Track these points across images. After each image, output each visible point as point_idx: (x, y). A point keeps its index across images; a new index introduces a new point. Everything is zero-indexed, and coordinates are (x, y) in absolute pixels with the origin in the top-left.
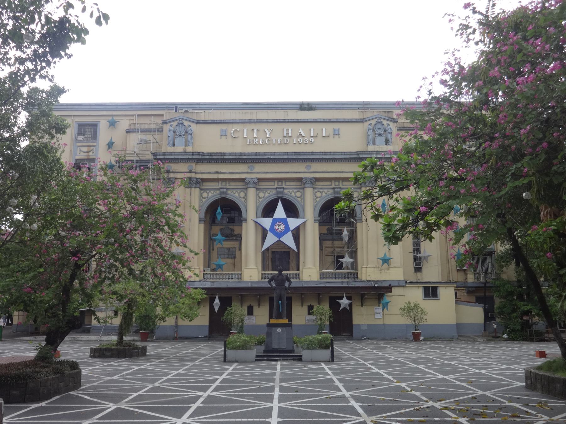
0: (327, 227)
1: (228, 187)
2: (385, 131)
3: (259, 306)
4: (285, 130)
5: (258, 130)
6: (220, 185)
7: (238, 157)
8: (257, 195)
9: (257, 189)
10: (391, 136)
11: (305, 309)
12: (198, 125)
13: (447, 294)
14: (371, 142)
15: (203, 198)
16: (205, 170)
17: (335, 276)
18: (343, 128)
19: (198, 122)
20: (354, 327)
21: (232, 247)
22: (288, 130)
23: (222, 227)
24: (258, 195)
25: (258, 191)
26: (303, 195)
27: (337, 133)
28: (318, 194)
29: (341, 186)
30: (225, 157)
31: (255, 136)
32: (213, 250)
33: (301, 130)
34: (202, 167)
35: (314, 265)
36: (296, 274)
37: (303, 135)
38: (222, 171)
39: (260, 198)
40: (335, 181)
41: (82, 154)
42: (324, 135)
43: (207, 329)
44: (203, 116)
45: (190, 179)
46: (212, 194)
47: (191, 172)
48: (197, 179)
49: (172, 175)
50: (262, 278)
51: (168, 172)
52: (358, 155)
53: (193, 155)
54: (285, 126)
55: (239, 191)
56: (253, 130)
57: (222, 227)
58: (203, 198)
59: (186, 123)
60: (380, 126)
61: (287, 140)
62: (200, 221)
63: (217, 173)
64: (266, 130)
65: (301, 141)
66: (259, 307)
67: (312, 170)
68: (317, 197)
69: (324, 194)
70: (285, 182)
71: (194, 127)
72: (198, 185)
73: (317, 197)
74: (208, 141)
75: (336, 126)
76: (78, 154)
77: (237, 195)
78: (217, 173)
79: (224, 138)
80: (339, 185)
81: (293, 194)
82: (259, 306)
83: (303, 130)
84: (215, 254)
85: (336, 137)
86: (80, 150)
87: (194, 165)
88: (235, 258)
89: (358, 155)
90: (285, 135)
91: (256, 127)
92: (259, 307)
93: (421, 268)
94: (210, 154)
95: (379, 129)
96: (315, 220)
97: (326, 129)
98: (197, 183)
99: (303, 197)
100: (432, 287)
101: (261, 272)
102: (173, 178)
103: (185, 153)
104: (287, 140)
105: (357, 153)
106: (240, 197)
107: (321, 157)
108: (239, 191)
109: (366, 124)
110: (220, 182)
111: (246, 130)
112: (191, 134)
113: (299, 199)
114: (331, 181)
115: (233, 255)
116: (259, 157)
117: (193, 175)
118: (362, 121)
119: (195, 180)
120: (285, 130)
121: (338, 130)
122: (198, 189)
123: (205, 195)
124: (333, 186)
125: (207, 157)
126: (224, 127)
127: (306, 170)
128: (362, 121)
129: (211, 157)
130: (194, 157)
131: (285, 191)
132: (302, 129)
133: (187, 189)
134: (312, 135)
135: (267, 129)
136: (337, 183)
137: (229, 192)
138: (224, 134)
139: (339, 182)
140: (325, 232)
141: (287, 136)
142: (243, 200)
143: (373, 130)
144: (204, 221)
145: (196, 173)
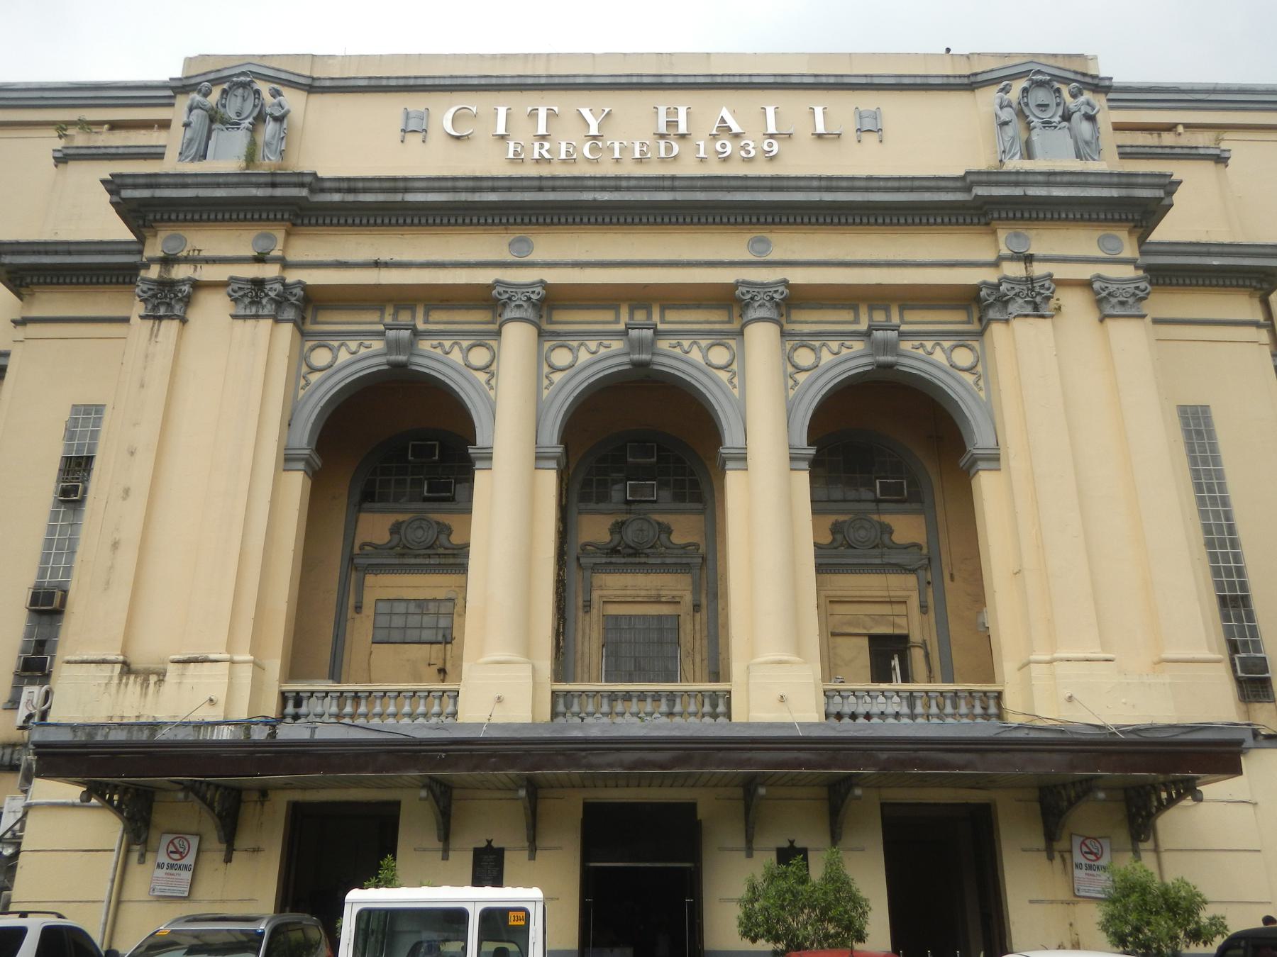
0: (833, 518)
1: (421, 326)
2: (1067, 117)
3: (533, 849)
4: (662, 110)
5: (551, 115)
6: (388, 319)
7: (463, 197)
8: (542, 358)
9: (541, 334)
10: (1096, 130)
12: (318, 100)
14: (1017, 148)
15: (314, 370)
16: (328, 259)
18: (891, 106)
21: (441, 594)
22: (672, 112)
23: (401, 517)
24: (547, 359)
25: (547, 345)
27: (870, 128)
28: (804, 357)
29: (895, 319)
30: (411, 197)
31: (542, 130)
32: (358, 608)
33: (725, 113)
34: (309, 247)
35: (798, 650)
36: (714, 696)
37: (736, 129)
38: (397, 258)
39: (555, 369)
40: (872, 308)
42: (820, 129)
45: (259, 284)
46: (352, 354)
47: (260, 259)
48: (284, 285)
49: (180, 272)
50: (554, 714)
51: (168, 261)
52: (968, 189)
53: (274, 185)
54: (663, 101)
55: (465, 344)
56: (533, 114)
57: (401, 517)
58: (314, 370)
60: (1041, 96)
61: (669, 149)
62: (288, 459)
63: (377, 264)
64: (586, 112)
65: (729, 150)
66: (532, 857)
67: (775, 255)
68: (800, 370)
69: (826, 357)
70: (663, 309)
71: (293, 100)
72: (290, 313)
73: (800, 370)
74: (344, 144)
75: (868, 101)
77: (456, 356)
78: (377, 264)
79: (414, 140)
80: (888, 318)
81: (696, 355)
82: (533, 849)
83: (734, 112)
84: (361, 629)
85: (870, 139)
88: (447, 639)
89: (968, 189)
90: (663, 129)
91: (543, 104)
92: (532, 857)
93: (1266, 683)
94: (350, 185)
95: (1043, 107)
96: (792, 459)
97: (822, 112)
98: (280, 302)
99: (737, 366)
101: (548, 686)
102: (183, 282)
104: (669, 149)
105: (967, 181)
106: (468, 366)
107: (815, 197)
108: (465, 344)
109: (988, 98)
110: (389, 311)
111: (500, 112)
112: (279, 119)
113: (724, 376)
114: (855, 308)
115: (439, 631)
116: (551, 196)
117: (269, 271)
118: (970, 84)
119: (278, 287)
120: (662, 110)
121: (875, 116)
122: (287, 330)
123: (321, 357)
124: (863, 326)
125: (337, 197)
126: (416, 103)
129: (350, 198)
130: (279, 192)
131: (664, 345)
132: (727, 110)
133: (240, 322)
134: (772, 129)
135: (590, 110)
136: (879, 317)
137: (425, 345)
138: (414, 128)
139: (887, 309)
140: (827, 539)
141: (671, 133)
142: (482, 377)
143: (1021, 114)
144: (308, 462)
145: (285, 264)
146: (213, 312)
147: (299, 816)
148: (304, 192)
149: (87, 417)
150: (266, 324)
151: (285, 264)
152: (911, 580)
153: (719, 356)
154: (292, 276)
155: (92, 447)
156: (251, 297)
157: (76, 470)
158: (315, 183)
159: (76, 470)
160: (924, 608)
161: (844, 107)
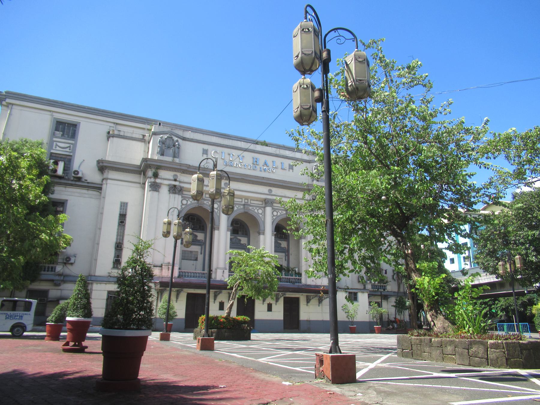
11: (265, 307)
13: (363, 297)
17: (289, 281)
19: (184, 139)
20: (301, 323)
21: (196, 250)
26: (264, 212)
41: (58, 148)
43: (184, 322)
44: (189, 135)
45: (175, 186)
47: (175, 180)
49: (158, 181)
59: (175, 139)
67: (273, 193)
73: (274, 216)
76: (54, 148)
85: (291, 170)
86: (57, 145)
87: (178, 174)
100: (354, 293)
103: (173, 162)
113: (261, 216)
117: (177, 183)
118: (309, 162)
126: (206, 147)
127: (268, 193)
128: (309, 162)
145: (180, 182)
146: (164, 190)
147: (189, 296)
148: (186, 168)
149: (124, 206)
150: (177, 196)
151: (180, 182)
152: (284, 254)
153: (260, 211)
154: (183, 185)
155: (126, 212)
156: (174, 189)
157: (122, 218)
158: (189, 166)
159: (122, 218)
160: (286, 260)
161: (287, 162)
